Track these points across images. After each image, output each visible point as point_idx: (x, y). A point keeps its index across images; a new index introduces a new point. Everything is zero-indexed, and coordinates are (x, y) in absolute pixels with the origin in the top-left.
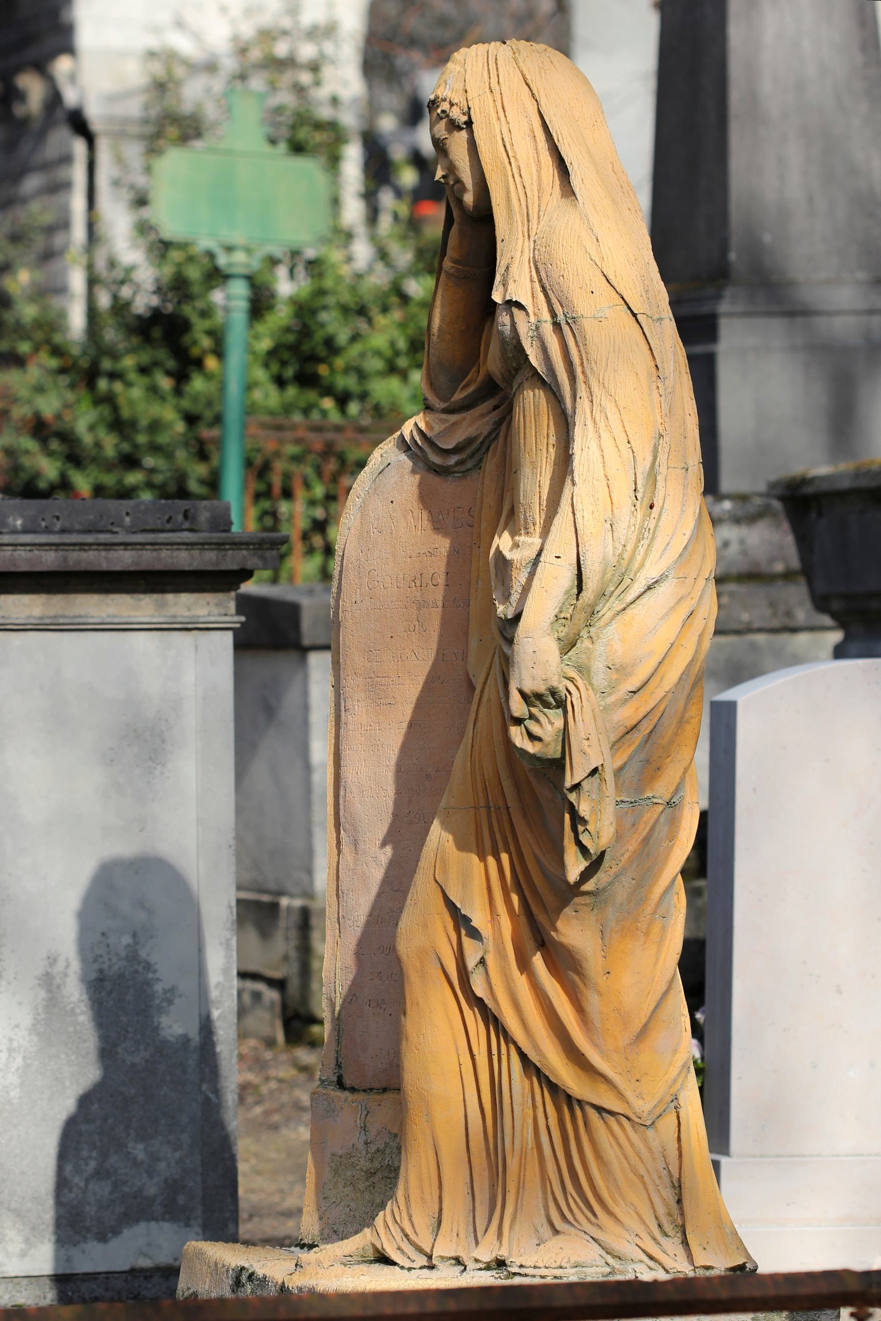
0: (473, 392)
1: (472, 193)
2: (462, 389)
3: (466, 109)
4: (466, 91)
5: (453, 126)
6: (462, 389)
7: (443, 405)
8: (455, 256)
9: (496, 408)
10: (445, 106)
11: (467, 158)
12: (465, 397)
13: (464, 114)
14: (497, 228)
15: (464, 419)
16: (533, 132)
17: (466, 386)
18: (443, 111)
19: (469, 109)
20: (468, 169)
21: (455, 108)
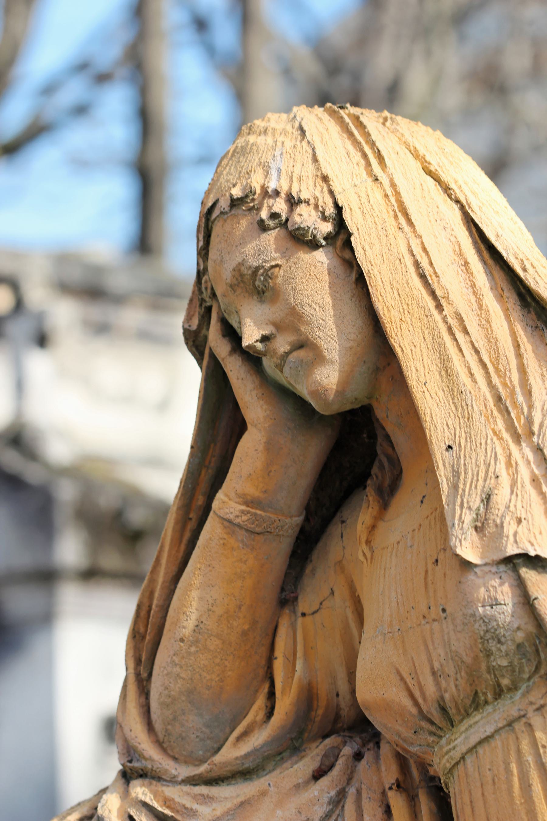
0: (266, 744)
1: (337, 367)
2: (239, 739)
3: (330, 210)
4: (325, 179)
5: (302, 240)
6: (239, 739)
7: (184, 771)
8: (252, 491)
9: (318, 775)
10: (280, 206)
11: (328, 302)
12: (247, 756)
13: (324, 218)
14: (427, 425)
15: (264, 794)
16: (461, 254)
17: (245, 734)
18: (274, 216)
19: (339, 209)
20: (330, 322)
21: (302, 209)
